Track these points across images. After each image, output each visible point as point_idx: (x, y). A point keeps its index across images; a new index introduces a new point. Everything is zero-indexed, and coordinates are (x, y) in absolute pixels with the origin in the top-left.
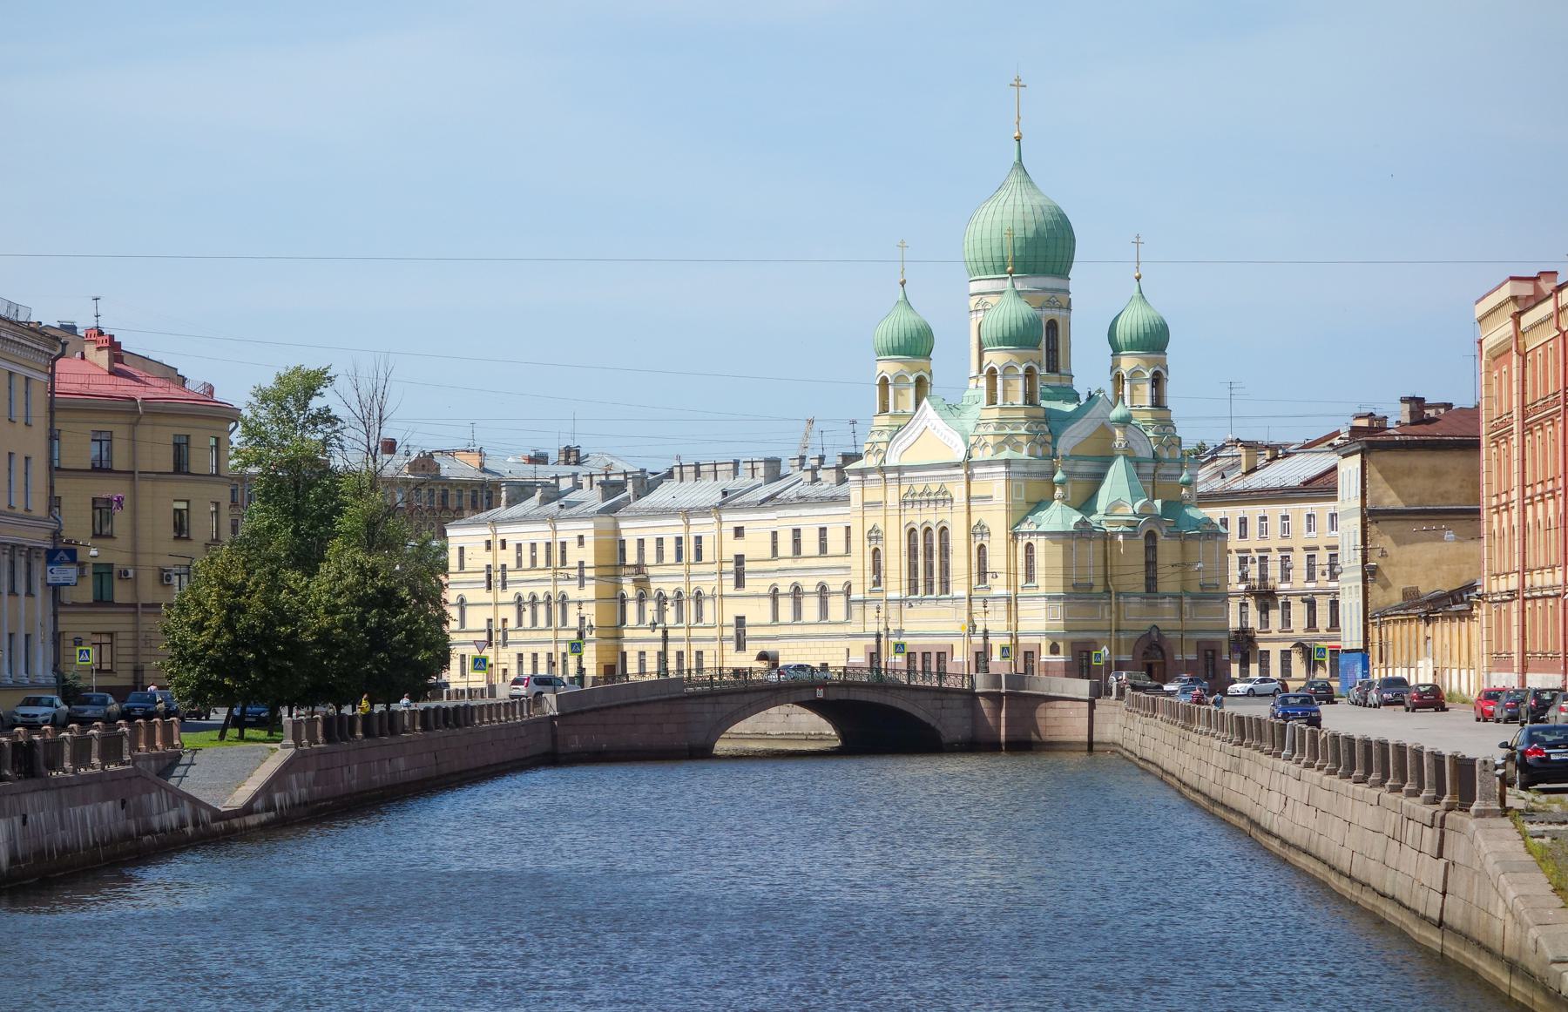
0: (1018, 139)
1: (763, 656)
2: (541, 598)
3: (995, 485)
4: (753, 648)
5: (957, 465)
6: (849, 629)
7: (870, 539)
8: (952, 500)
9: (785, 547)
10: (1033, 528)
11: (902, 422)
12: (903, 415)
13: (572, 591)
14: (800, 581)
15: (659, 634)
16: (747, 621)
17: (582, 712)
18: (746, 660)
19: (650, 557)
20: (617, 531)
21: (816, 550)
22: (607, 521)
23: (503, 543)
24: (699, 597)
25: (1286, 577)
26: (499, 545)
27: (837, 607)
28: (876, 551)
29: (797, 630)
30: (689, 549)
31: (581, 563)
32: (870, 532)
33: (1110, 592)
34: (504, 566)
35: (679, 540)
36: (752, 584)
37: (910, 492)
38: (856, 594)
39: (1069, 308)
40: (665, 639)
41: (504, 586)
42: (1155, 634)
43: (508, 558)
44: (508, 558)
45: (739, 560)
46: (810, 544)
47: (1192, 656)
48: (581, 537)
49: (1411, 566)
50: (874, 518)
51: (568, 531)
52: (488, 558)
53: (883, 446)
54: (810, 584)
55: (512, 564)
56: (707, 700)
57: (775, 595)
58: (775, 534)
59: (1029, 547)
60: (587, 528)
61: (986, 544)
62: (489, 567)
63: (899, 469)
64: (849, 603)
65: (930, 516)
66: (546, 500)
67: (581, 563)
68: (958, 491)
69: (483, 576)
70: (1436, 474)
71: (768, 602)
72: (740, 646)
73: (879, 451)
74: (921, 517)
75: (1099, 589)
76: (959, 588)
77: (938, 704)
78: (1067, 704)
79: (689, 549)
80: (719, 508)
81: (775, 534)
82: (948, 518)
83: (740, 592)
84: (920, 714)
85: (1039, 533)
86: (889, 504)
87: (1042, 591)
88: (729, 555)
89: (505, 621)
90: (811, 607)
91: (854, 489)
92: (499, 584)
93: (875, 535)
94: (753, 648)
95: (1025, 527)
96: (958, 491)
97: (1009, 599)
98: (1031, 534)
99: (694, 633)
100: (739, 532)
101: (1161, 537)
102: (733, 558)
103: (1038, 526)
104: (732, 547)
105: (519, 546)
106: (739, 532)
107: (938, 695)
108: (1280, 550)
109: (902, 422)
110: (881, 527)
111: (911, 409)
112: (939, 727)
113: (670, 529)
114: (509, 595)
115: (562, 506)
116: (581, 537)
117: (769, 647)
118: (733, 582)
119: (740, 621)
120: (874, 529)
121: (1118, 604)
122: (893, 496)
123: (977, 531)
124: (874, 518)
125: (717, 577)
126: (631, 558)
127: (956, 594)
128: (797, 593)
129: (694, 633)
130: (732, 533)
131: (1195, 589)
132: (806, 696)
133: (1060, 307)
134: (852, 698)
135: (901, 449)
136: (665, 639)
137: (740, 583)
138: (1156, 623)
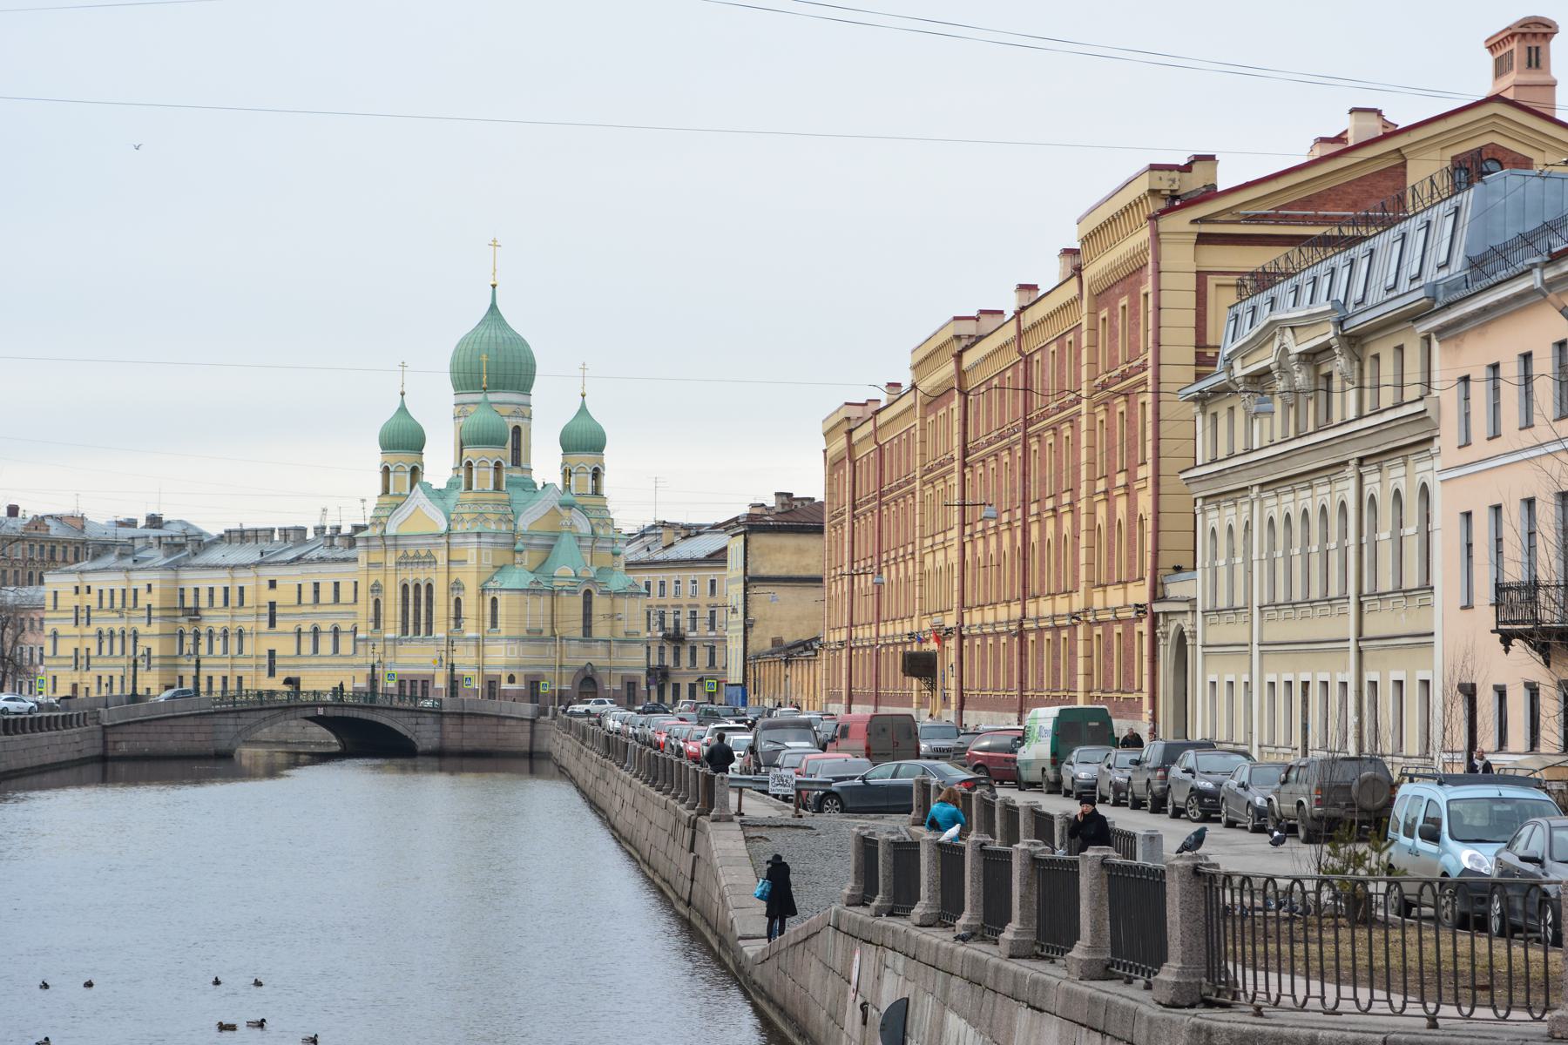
0: (494, 286)
1: (288, 681)
2: (117, 632)
3: (471, 554)
4: (281, 674)
5: (441, 536)
6: (356, 661)
7: (372, 591)
8: (436, 562)
9: (308, 596)
10: (498, 586)
11: (399, 501)
12: (400, 495)
13: (142, 628)
14: (318, 622)
15: (193, 662)
16: (277, 653)
17: (129, 723)
18: (276, 684)
19: (204, 602)
20: (177, 581)
21: (331, 599)
22: (169, 575)
23: (89, 588)
24: (241, 634)
25: (694, 628)
26: (85, 590)
27: (346, 645)
28: (377, 602)
29: (315, 661)
30: (234, 596)
31: (149, 606)
32: (373, 586)
33: (555, 636)
34: (88, 607)
35: (226, 589)
36: (279, 626)
37: (405, 556)
38: (359, 635)
39: (530, 418)
40: (198, 666)
41: (88, 624)
42: (589, 669)
43: (92, 601)
44: (92, 601)
45: (272, 605)
46: (326, 594)
47: (618, 687)
48: (149, 586)
49: (780, 621)
50: (376, 576)
51: (140, 580)
52: (76, 601)
53: (384, 520)
54: (326, 626)
55: (95, 604)
56: (231, 715)
57: (299, 633)
58: (300, 586)
59: (494, 600)
60: (154, 578)
61: (462, 598)
62: (77, 607)
63: (396, 537)
64: (355, 640)
65: (420, 575)
66: (122, 556)
67: (149, 606)
68: (441, 556)
69: (73, 615)
70: (800, 551)
71: (295, 639)
72: (272, 673)
75: (547, 633)
76: (440, 631)
77: (414, 721)
78: (513, 723)
79: (234, 596)
80: (258, 565)
82: (433, 577)
83: (272, 630)
84: (399, 728)
85: (501, 590)
86: (388, 565)
87: (503, 634)
89: (88, 649)
90: (326, 644)
91: (360, 552)
92: (85, 621)
93: (376, 588)
94: (281, 674)
95: (491, 585)
96: (441, 556)
97: (477, 639)
98: (495, 589)
99: (238, 662)
100: (273, 584)
101: (595, 595)
103: (501, 584)
104: (270, 595)
105: (101, 591)
106: (273, 584)
107: (414, 714)
108: (690, 606)
109: (399, 501)
110: (381, 582)
111: (408, 492)
112: (414, 739)
113: (219, 580)
114: (92, 630)
115: (135, 561)
116: (149, 586)
117: (293, 674)
118: (267, 625)
119: (272, 653)
120: (376, 584)
121: (561, 646)
122: (391, 559)
123: (456, 586)
124: (376, 576)
125: (254, 619)
126: (189, 603)
127: (438, 635)
128: (316, 632)
129: (238, 662)
130: (267, 584)
131: (622, 636)
132: (310, 713)
133: (523, 417)
134: (346, 715)
135: (399, 522)
136: (198, 666)
137: (272, 624)
138: (590, 660)
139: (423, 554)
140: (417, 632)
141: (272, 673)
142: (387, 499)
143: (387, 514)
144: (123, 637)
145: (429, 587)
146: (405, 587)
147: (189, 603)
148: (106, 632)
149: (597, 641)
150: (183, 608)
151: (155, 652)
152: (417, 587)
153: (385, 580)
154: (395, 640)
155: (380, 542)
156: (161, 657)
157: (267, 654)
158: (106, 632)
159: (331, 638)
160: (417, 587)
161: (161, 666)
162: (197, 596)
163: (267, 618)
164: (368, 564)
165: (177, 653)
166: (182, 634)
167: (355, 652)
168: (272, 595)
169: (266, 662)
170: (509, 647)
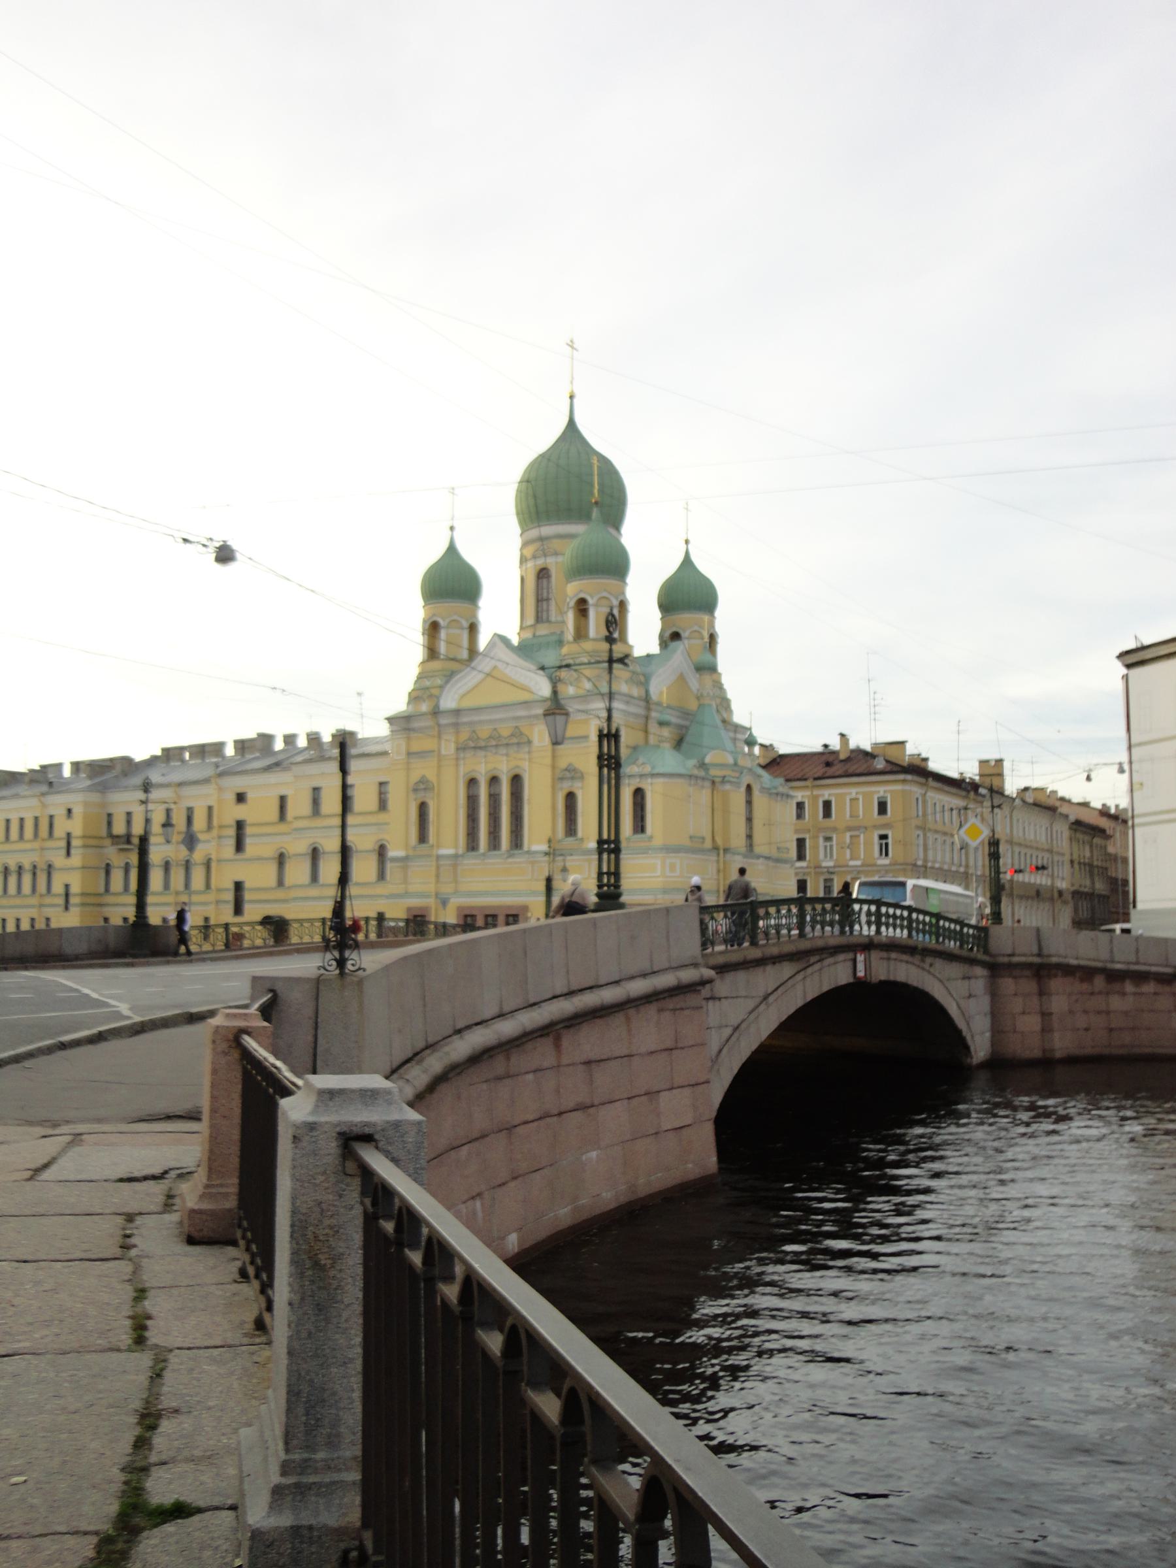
0: (571, 397)
8: (529, 742)
10: (648, 769)
11: (454, 666)
13: (59, 860)
16: (247, 885)
28: (423, 808)
45: (240, 825)
48: (69, 811)
50: (425, 769)
53: (435, 692)
63: (457, 712)
67: (69, 835)
71: (273, 868)
73: (431, 696)
74: (481, 768)
75: (708, 844)
81: (283, 800)
82: (525, 765)
83: (239, 856)
87: (658, 841)
88: (230, 820)
98: (642, 776)
102: (234, 824)
106: (241, 798)
116: (69, 811)
117: (274, 910)
119: (238, 886)
126: (119, 828)
127: (535, 848)
130: (233, 797)
135: (461, 692)
137: (239, 846)
139: (505, 733)
140: (494, 843)
141: (238, 910)
142: (435, 665)
143: (439, 682)
144: (34, 874)
145: (516, 780)
146: (472, 782)
147: (119, 828)
148: (13, 867)
149: (758, 857)
150: (111, 835)
151: (75, 889)
152: (494, 780)
153: (439, 775)
154: (456, 856)
155: (428, 722)
156: (83, 894)
157: (231, 886)
158: (13, 867)
159: (306, 866)
160: (494, 780)
161: (83, 905)
162: (129, 822)
163: (232, 842)
164: (409, 754)
165: (102, 889)
166: (108, 869)
167: (381, 875)
168: (241, 812)
169: (230, 896)
170: (668, 861)
